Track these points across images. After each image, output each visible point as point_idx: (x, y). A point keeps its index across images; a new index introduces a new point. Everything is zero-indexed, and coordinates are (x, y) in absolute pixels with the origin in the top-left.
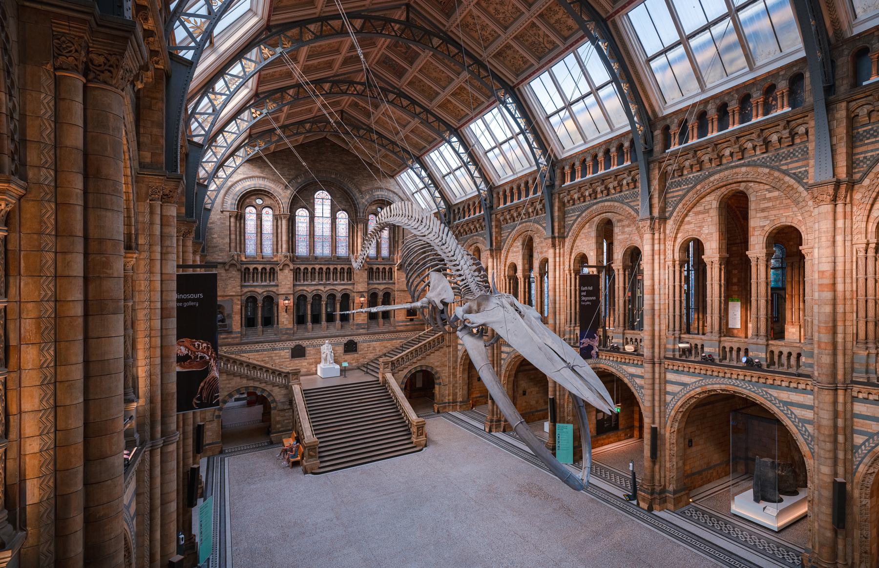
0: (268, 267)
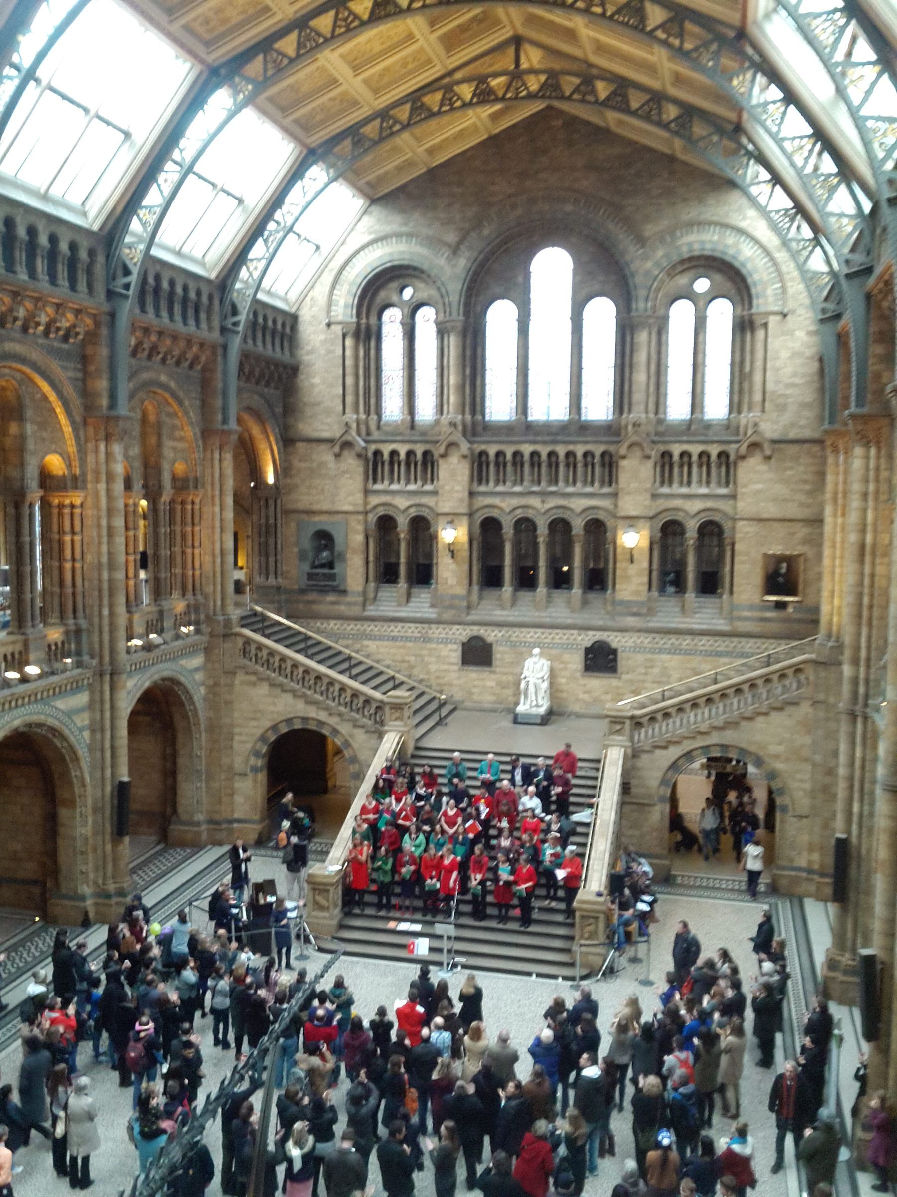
0: (419, 450)
